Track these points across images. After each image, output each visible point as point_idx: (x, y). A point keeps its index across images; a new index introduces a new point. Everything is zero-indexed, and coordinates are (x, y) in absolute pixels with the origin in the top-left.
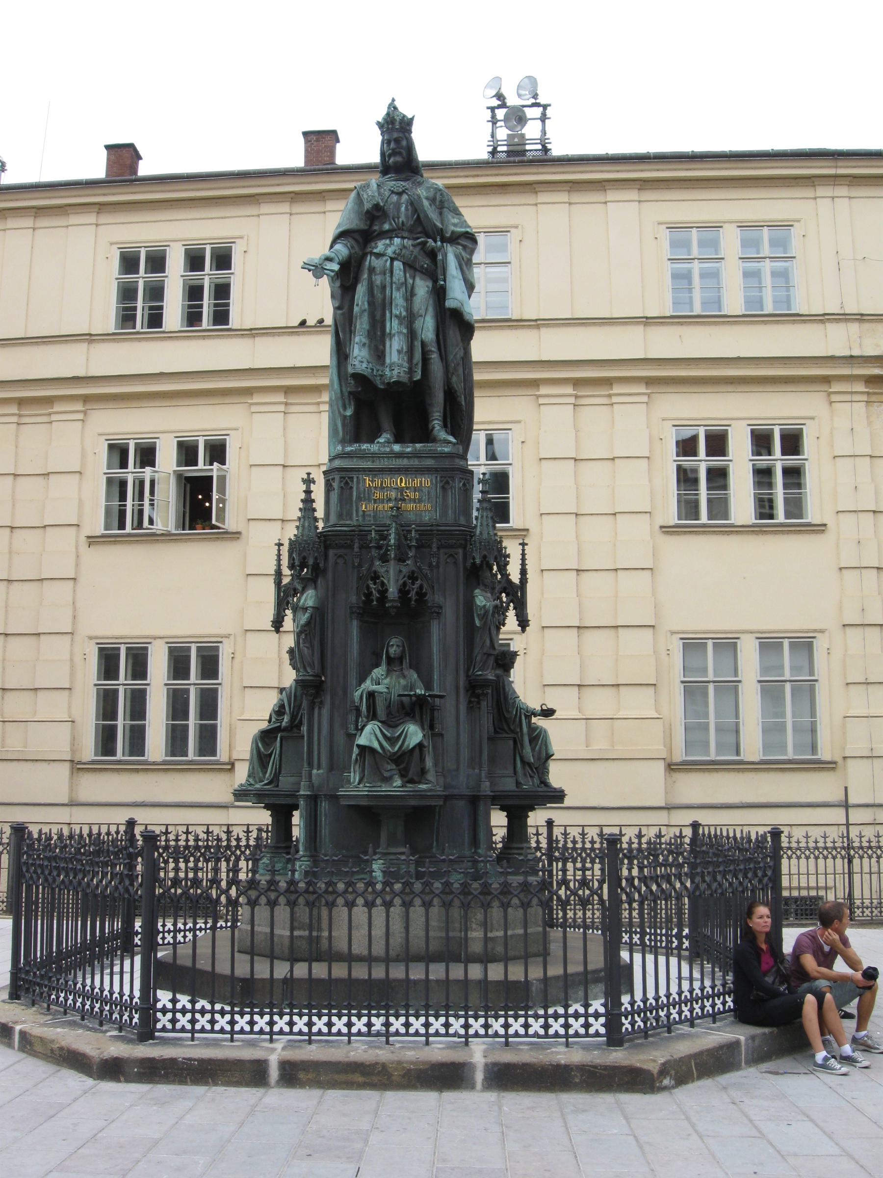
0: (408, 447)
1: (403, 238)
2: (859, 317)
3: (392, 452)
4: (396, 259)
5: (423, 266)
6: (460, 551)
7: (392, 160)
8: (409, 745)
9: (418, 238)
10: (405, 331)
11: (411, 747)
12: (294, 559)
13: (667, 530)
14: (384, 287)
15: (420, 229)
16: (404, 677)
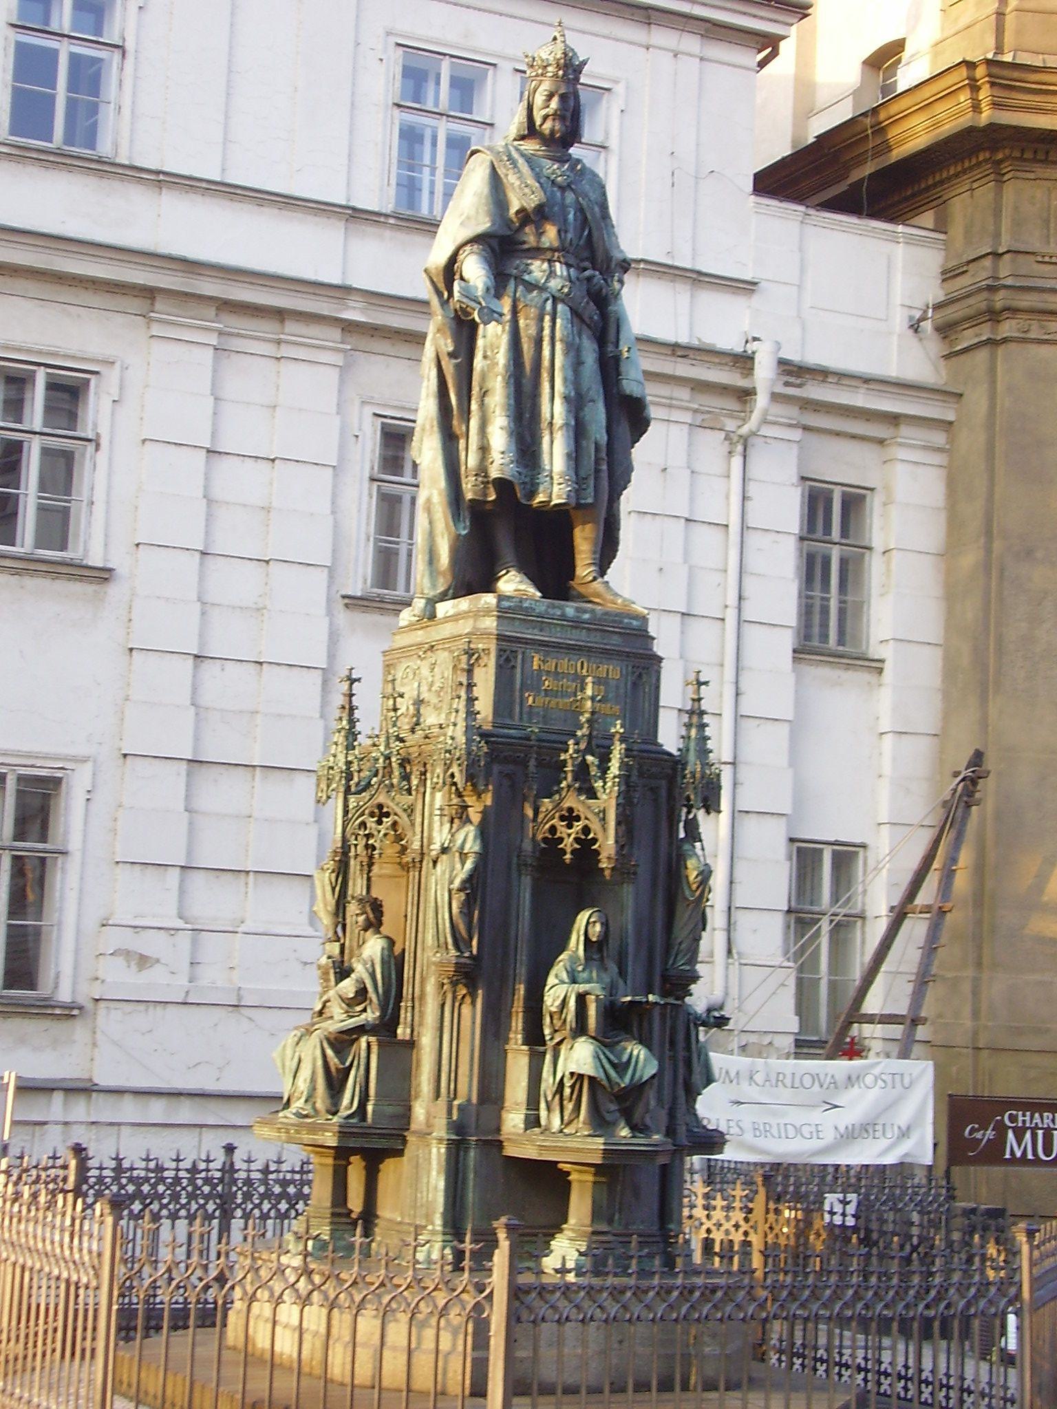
0: (585, 611)
1: (569, 266)
2: (694, 276)
3: (563, 617)
4: (563, 301)
5: (591, 318)
6: (664, 783)
7: (548, 126)
8: (641, 1077)
9: (585, 269)
10: (573, 423)
11: (645, 1078)
12: (452, 776)
13: (354, 603)
14: (539, 342)
15: (586, 254)
16: (606, 969)
